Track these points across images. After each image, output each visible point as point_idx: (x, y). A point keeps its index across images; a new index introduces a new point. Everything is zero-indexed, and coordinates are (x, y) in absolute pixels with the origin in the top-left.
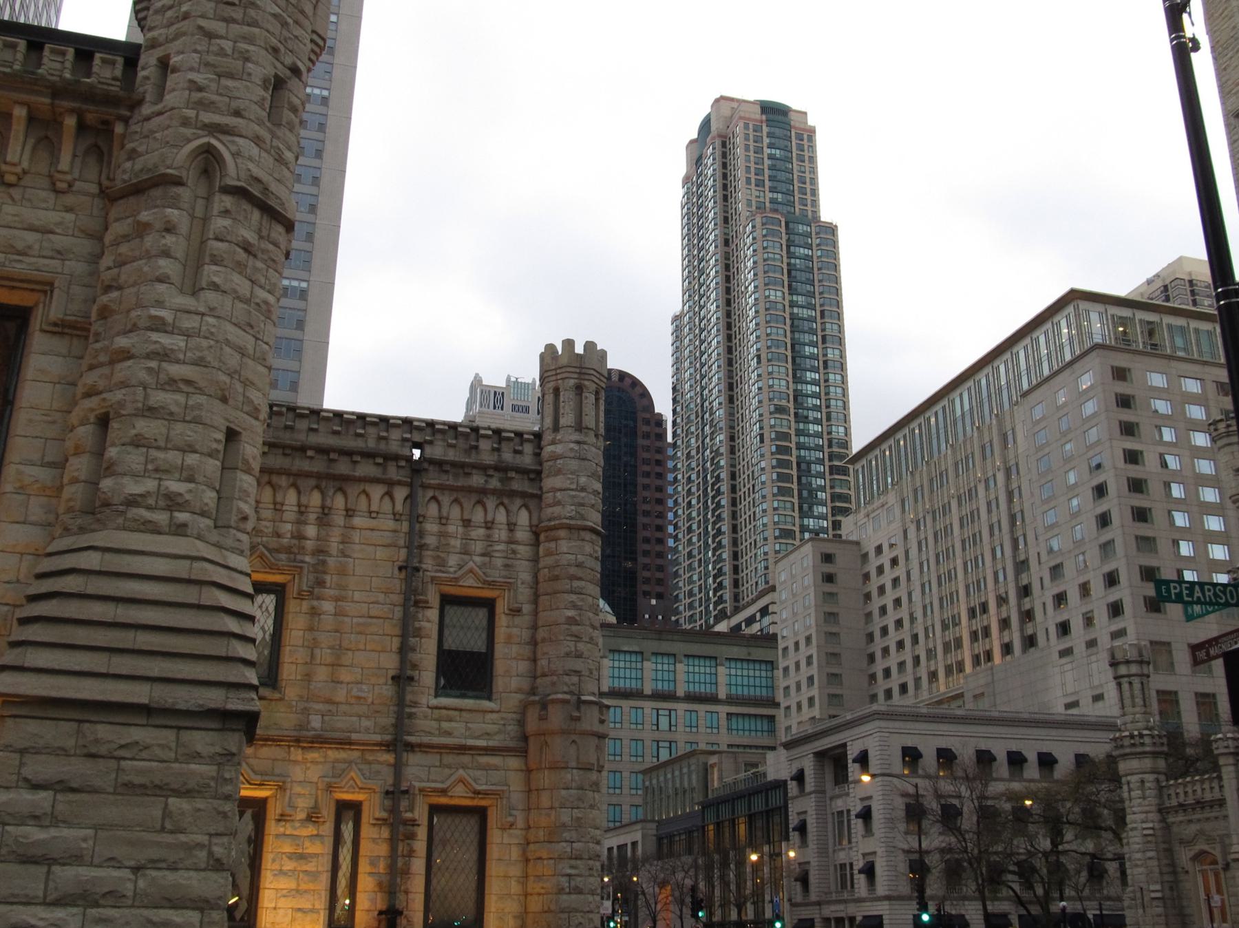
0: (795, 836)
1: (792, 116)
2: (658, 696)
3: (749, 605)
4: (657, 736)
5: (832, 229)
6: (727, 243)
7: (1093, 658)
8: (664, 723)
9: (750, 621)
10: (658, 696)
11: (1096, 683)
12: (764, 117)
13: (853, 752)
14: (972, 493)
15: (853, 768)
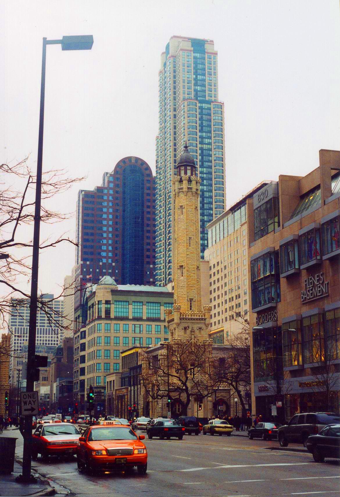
2: (135, 319)
4: (134, 335)
6: (175, 110)
8: (137, 330)
10: (135, 319)
12: (192, 49)
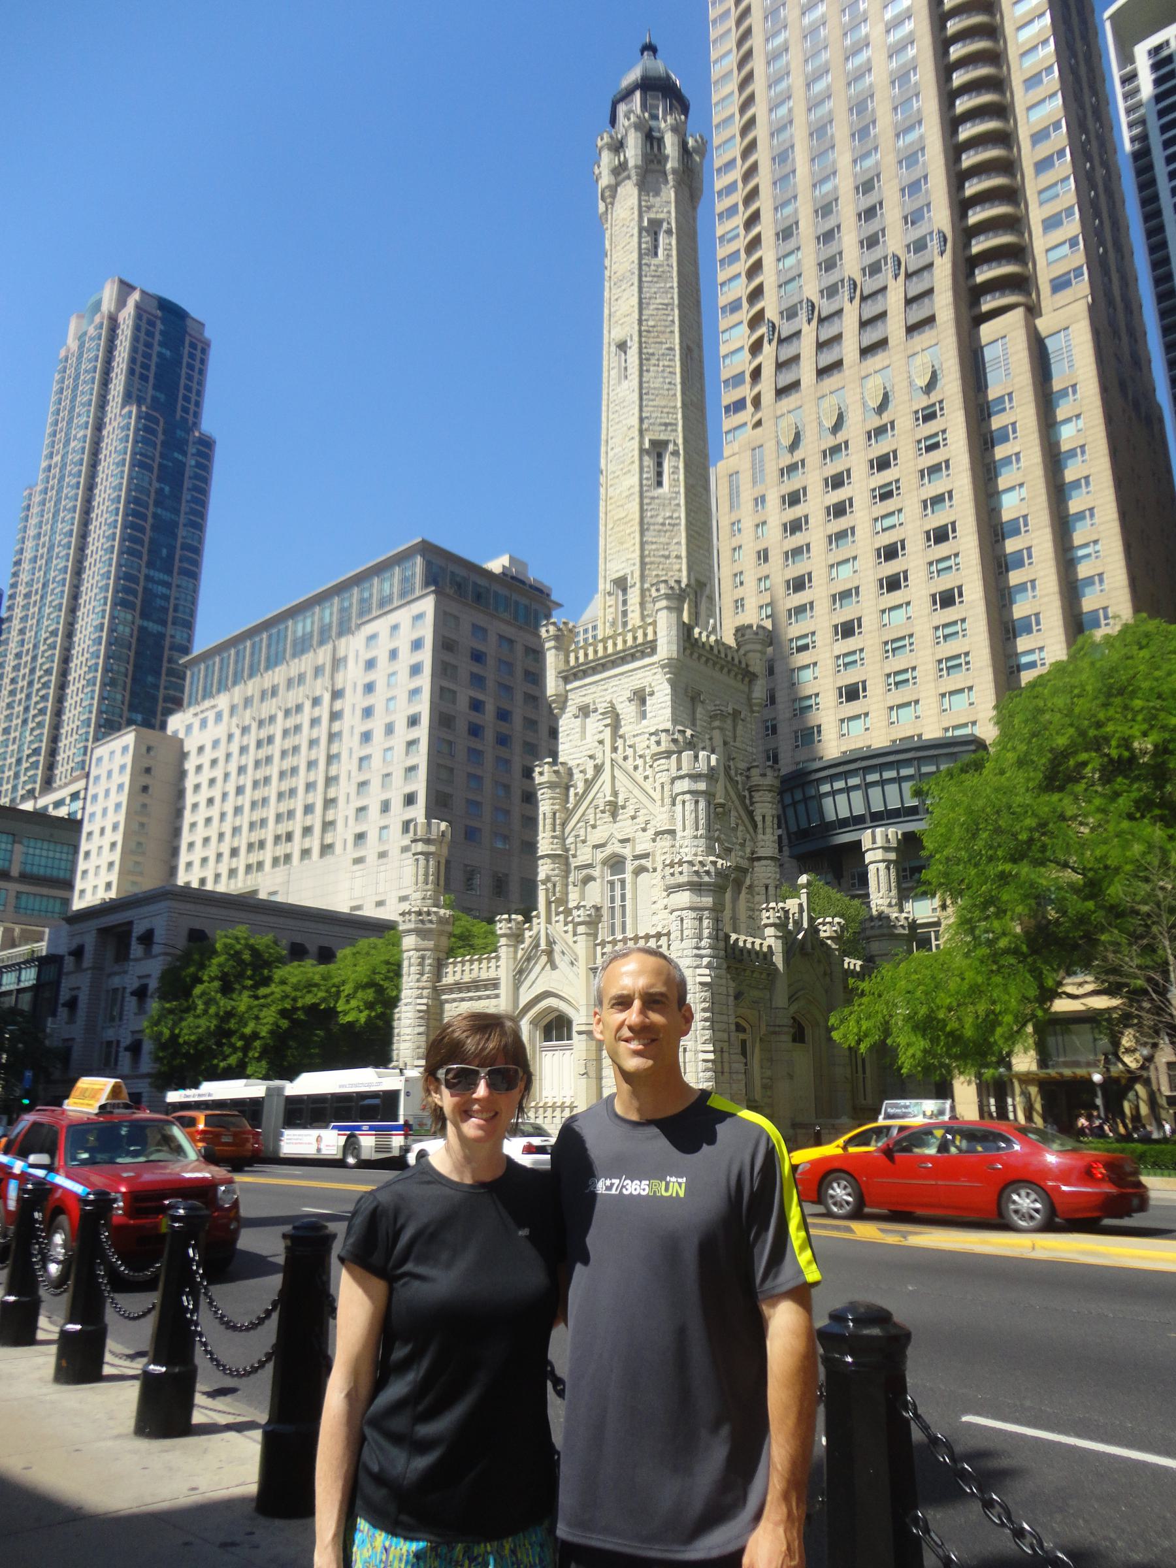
0: (63, 1012)
1: (189, 322)
3: (61, 787)
5: (207, 445)
7: (382, 868)
9: (58, 804)
11: (381, 890)
13: (138, 929)
14: (299, 708)
15: (136, 950)
